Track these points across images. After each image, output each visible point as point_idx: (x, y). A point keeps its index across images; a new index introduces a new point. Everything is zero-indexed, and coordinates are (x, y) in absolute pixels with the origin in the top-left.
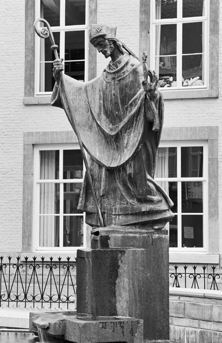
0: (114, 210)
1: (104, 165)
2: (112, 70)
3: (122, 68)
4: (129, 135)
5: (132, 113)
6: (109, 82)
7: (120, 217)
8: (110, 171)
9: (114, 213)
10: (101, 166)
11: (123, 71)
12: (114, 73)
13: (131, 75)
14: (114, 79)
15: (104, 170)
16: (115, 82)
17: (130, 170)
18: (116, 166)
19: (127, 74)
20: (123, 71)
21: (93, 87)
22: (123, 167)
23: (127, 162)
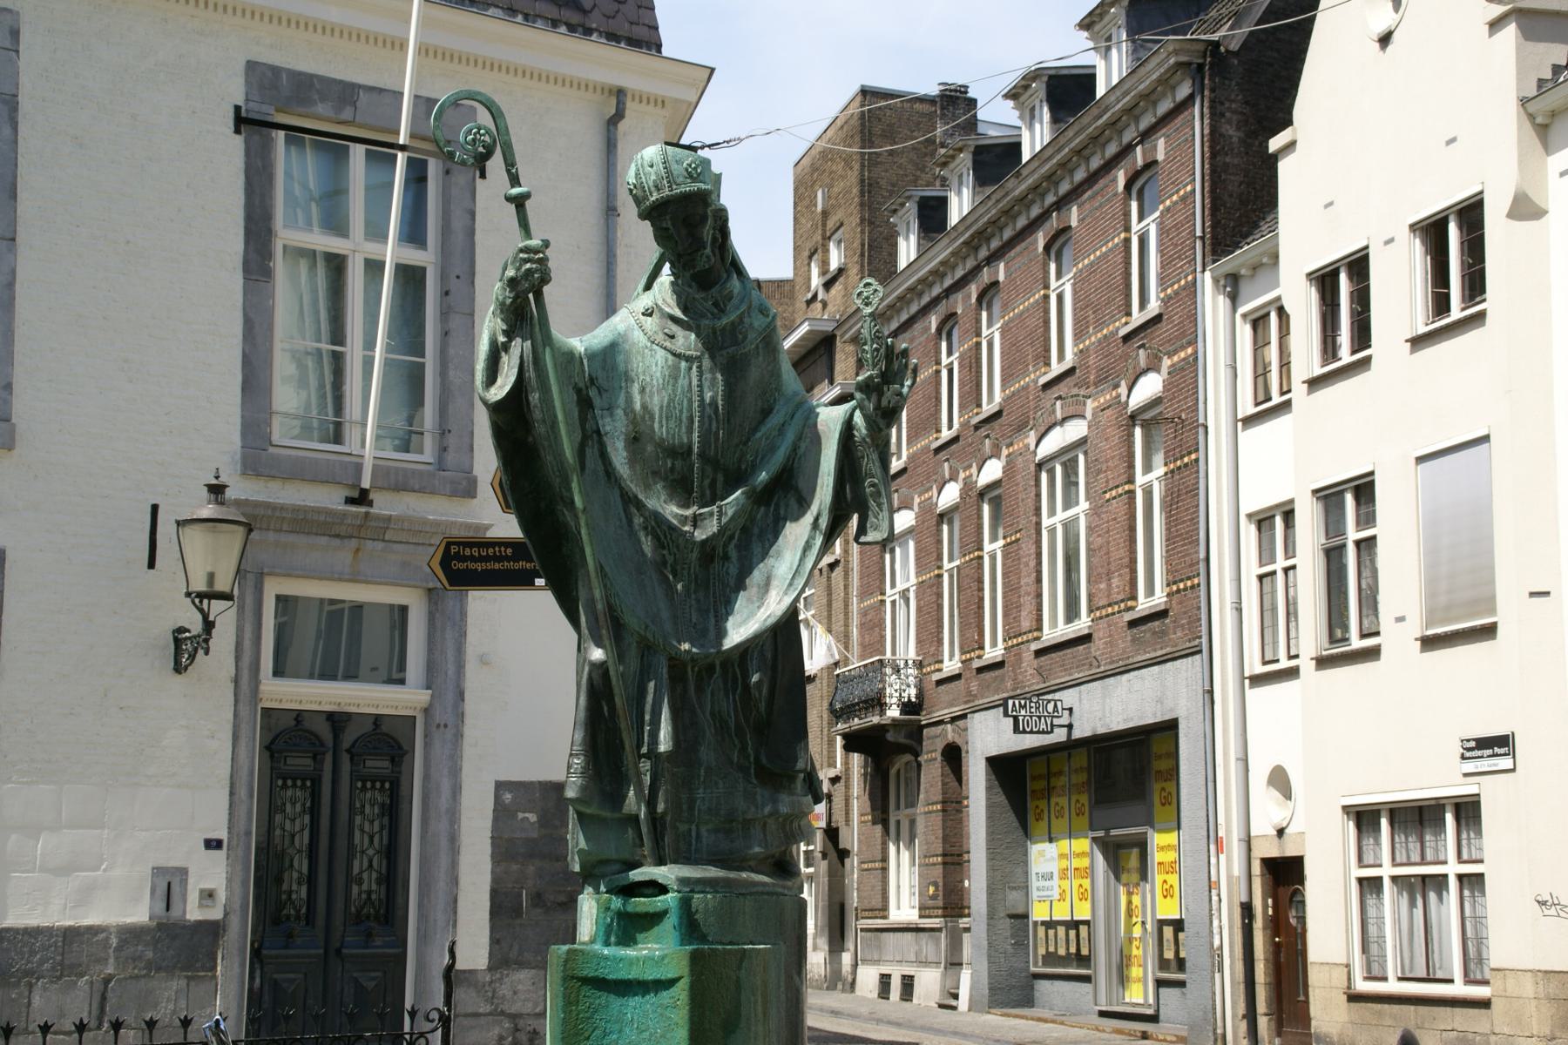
0: (685, 807)
13: (760, 346)
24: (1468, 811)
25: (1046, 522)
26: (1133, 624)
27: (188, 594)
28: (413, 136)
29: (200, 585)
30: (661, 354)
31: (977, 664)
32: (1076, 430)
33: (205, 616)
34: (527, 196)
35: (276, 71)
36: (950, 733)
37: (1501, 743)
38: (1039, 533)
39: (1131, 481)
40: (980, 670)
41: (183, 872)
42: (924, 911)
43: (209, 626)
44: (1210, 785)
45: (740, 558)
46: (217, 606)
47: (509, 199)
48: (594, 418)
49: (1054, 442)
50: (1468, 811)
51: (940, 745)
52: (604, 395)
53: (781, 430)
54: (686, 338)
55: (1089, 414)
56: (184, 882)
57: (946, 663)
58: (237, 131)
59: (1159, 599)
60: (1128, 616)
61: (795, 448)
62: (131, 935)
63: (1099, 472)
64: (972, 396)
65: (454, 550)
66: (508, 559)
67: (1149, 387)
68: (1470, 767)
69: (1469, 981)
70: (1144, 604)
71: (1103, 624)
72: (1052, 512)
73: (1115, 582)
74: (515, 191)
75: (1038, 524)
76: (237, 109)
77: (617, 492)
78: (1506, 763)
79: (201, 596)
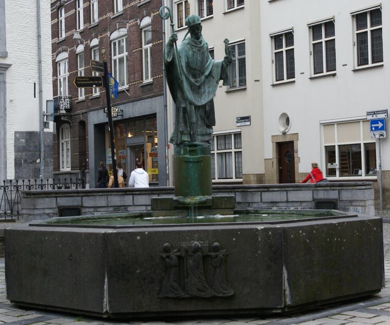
4: (204, 86)
8: (197, 108)
12: (200, 47)
18: (200, 104)
22: (204, 106)
23: (208, 103)
24: (238, 135)
25: (113, 58)
26: (142, 87)
30: (191, 52)
31: (90, 98)
32: (124, 31)
34: (174, 25)
36: (82, 118)
37: (247, 118)
38: (111, 61)
39: (141, 47)
40: (91, 99)
42: (73, 168)
44: (166, 131)
49: (115, 35)
50: (238, 135)
51: (78, 121)
53: (209, 64)
55: (127, 27)
57: (79, 97)
59: (150, 80)
60: (140, 85)
61: (212, 68)
63: (131, 44)
64: (88, 19)
65: (77, 79)
66: (88, 81)
67: (147, 21)
68: (239, 124)
69: (236, 178)
70: (145, 81)
71: (132, 87)
72: (115, 55)
73: (136, 75)
75: (111, 58)
78: (248, 123)
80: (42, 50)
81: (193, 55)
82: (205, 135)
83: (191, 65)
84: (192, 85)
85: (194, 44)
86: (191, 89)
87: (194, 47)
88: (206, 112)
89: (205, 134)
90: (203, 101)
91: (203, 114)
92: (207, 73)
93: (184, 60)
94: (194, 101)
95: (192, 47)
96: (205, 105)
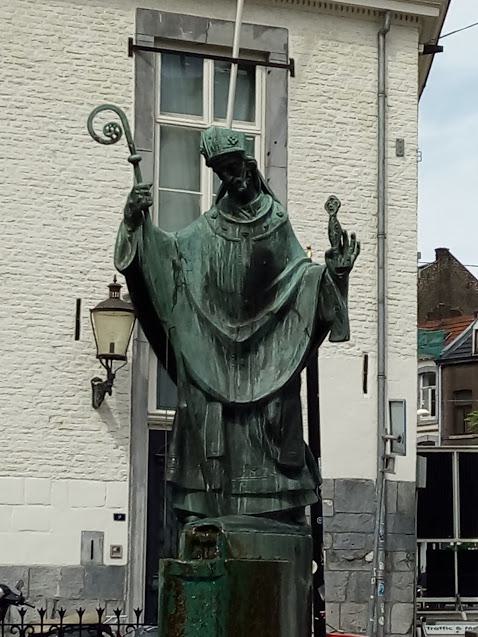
1: (219, 399)
2: (244, 219)
3: (264, 218)
4: (268, 346)
5: (275, 306)
6: (234, 241)
7: (245, 499)
8: (234, 413)
9: (234, 492)
10: (211, 397)
11: (265, 224)
12: (248, 225)
14: (246, 235)
15: (219, 407)
16: (248, 241)
17: (272, 410)
19: (271, 230)
20: (265, 224)
21: (189, 244)
22: (259, 407)
27: (98, 357)
28: (241, 51)
29: (107, 352)
33: (109, 369)
34: (139, 160)
35: (155, 13)
41: (101, 534)
43: (111, 377)
45: (266, 353)
46: (115, 364)
47: (130, 160)
48: (183, 275)
52: (189, 263)
53: (289, 277)
54: (234, 230)
56: (102, 542)
58: (130, 55)
62: (68, 573)
74: (134, 156)
76: (131, 40)
77: (196, 316)
79: (107, 357)
80: (390, 270)
81: (227, 248)
82: (269, 496)
83: (220, 282)
84: (219, 341)
85: (229, 217)
86: (220, 353)
87: (230, 227)
88: (270, 429)
89: (263, 491)
90: (257, 390)
91: (259, 431)
92: (280, 301)
93: (198, 264)
94: (220, 388)
95: (225, 223)
96: (265, 401)
